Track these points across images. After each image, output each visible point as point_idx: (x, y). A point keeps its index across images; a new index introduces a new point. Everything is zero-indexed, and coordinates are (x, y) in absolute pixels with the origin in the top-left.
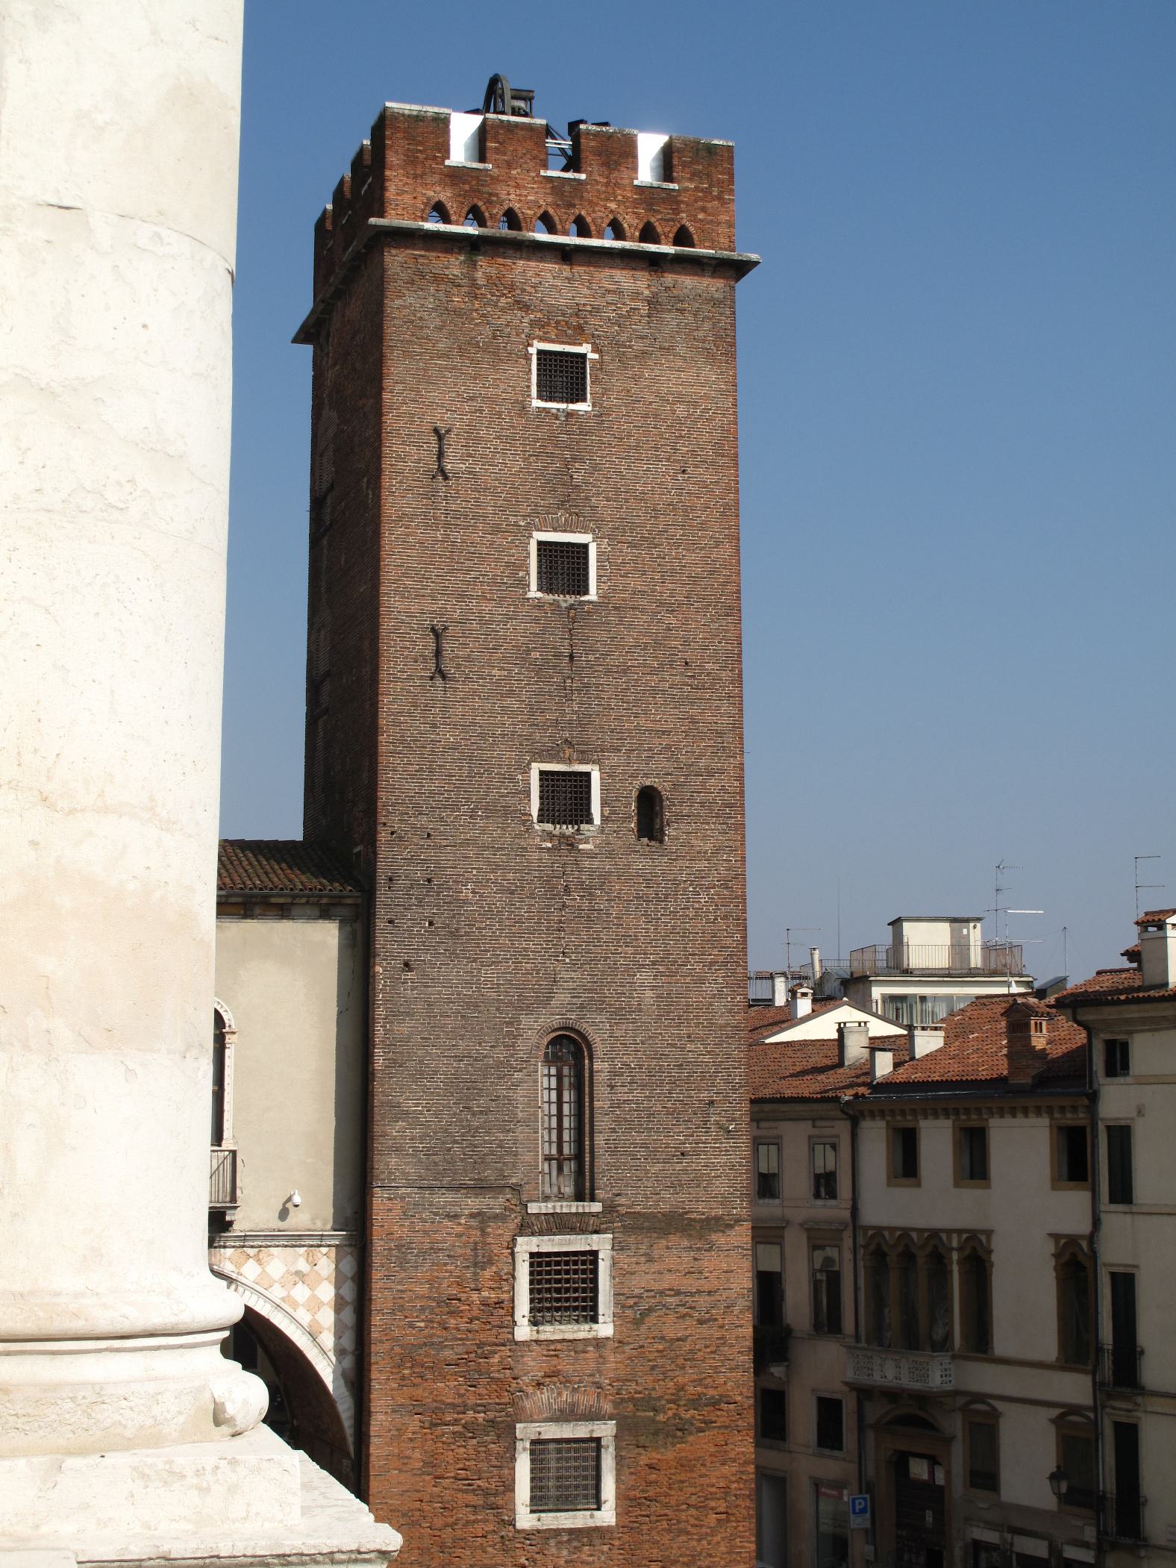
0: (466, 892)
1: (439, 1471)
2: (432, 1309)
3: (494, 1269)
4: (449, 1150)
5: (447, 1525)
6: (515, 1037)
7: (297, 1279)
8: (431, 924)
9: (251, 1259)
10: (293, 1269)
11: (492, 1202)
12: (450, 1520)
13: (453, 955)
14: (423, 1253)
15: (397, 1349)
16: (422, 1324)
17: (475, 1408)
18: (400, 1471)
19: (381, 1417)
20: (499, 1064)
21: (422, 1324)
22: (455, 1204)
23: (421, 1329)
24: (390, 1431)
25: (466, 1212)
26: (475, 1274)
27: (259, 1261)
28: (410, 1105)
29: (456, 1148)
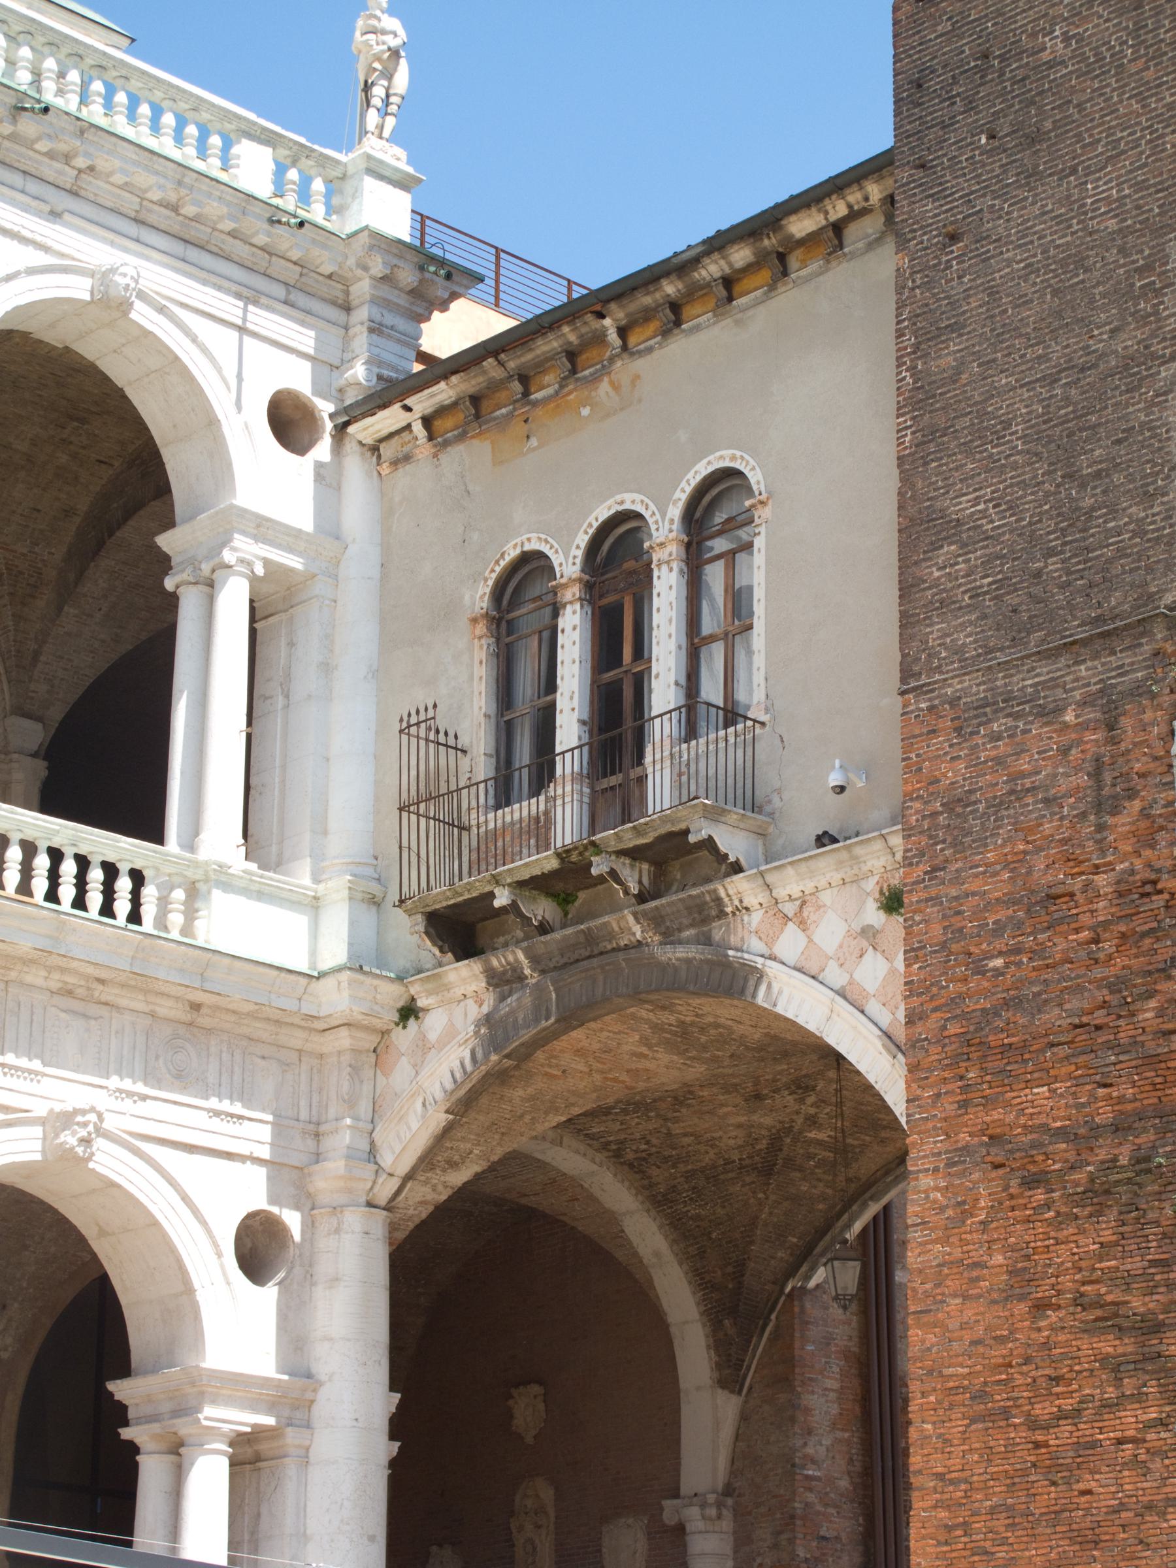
0: (1054, 46)
1: (1044, 1291)
2: (1020, 924)
3: (1137, 804)
4: (1038, 574)
5: (1061, 1416)
6: (1158, 292)
7: (865, 944)
8: (992, 137)
9: (790, 924)
10: (857, 926)
11: (1127, 659)
12: (1068, 1404)
13: (1031, 176)
14: (997, 805)
15: (953, 1029)
16: (998, 962)
17: (1118, 1128)
18: (966, 1297)
19: (926, 1181)
20: (1127, 363)
21: (998, 962)
22: (1052, 684)
23: (998, 972)
24: (942, 1209)
25: (1077, 695)
26: (1101, 828)
27: (803, 925)
28: (963, 506)
29: (1053, 565)
